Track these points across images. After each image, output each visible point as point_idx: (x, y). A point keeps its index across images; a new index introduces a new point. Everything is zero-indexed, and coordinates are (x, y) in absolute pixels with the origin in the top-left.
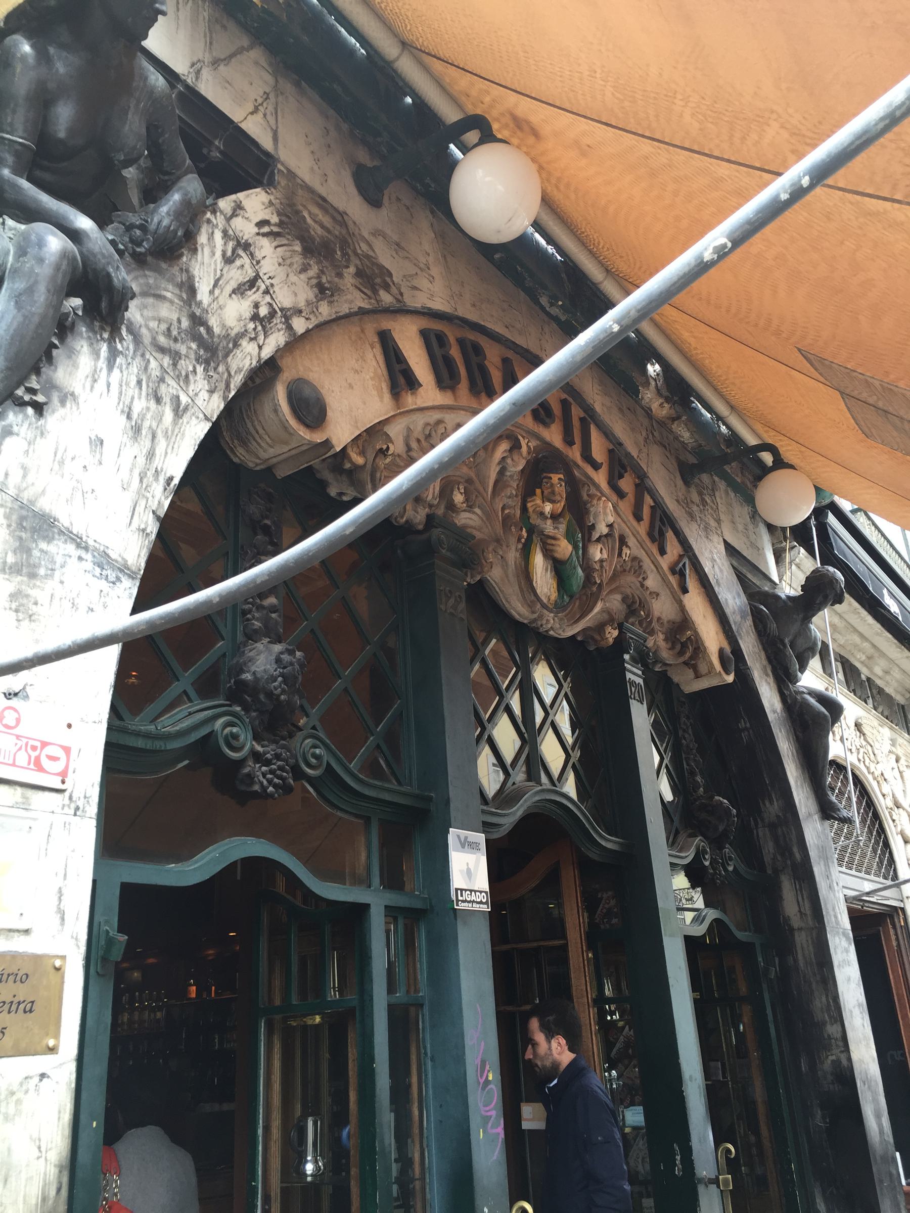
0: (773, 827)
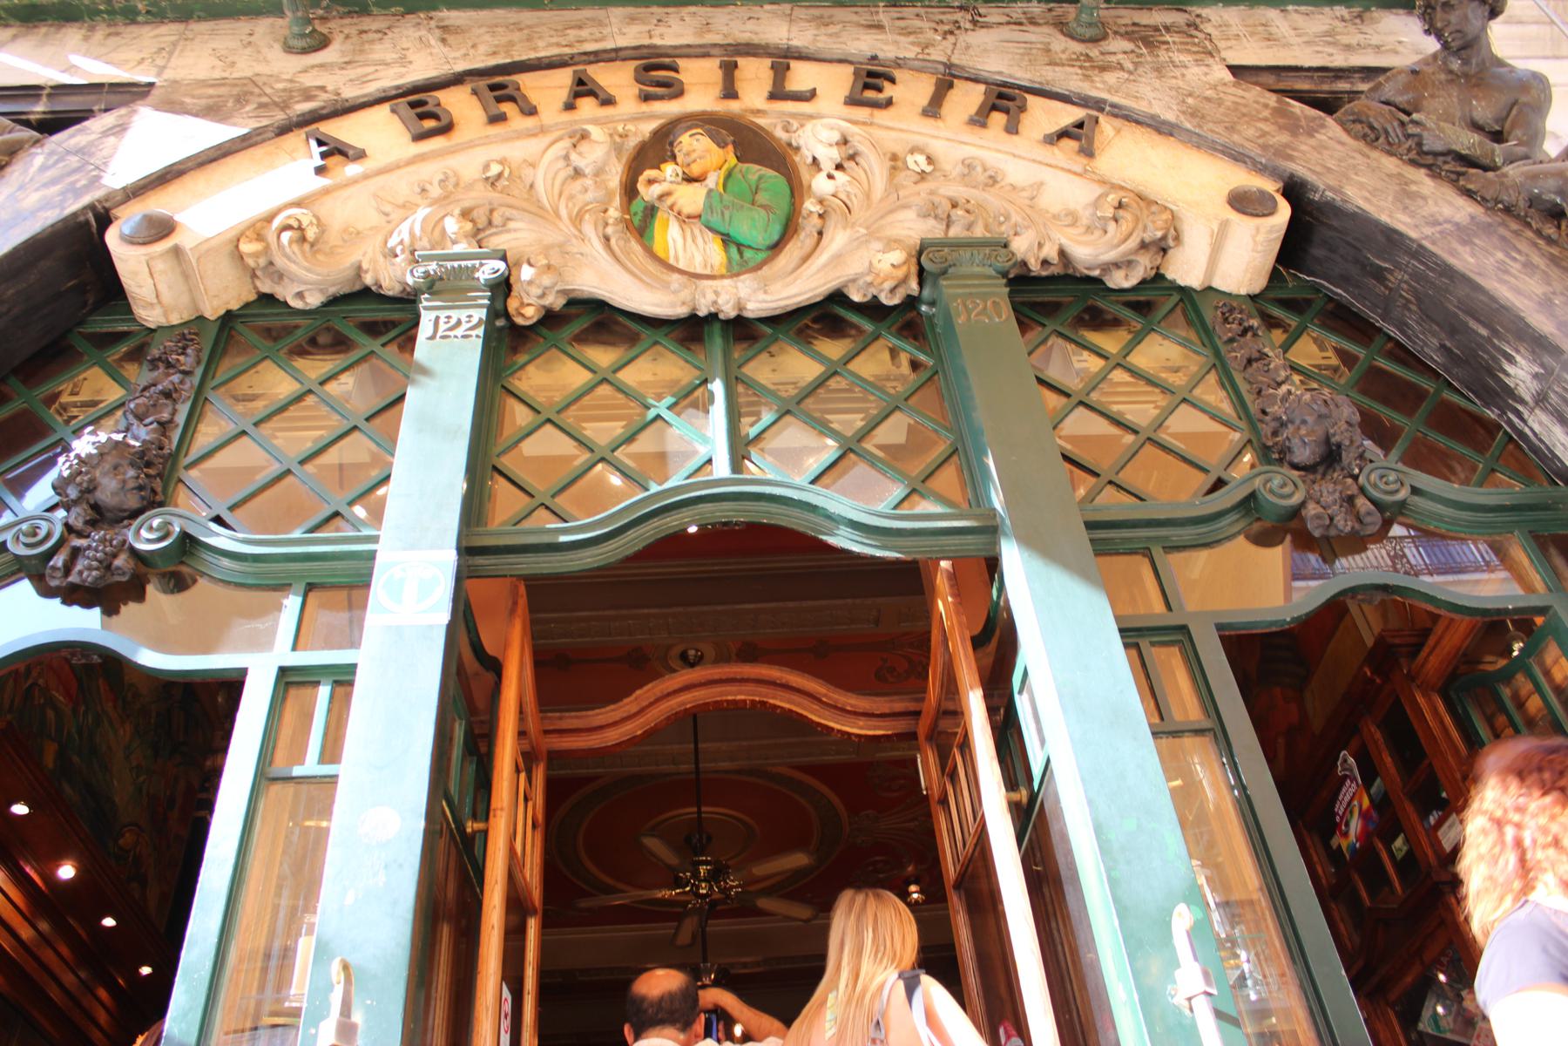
0: (1541, 400)
